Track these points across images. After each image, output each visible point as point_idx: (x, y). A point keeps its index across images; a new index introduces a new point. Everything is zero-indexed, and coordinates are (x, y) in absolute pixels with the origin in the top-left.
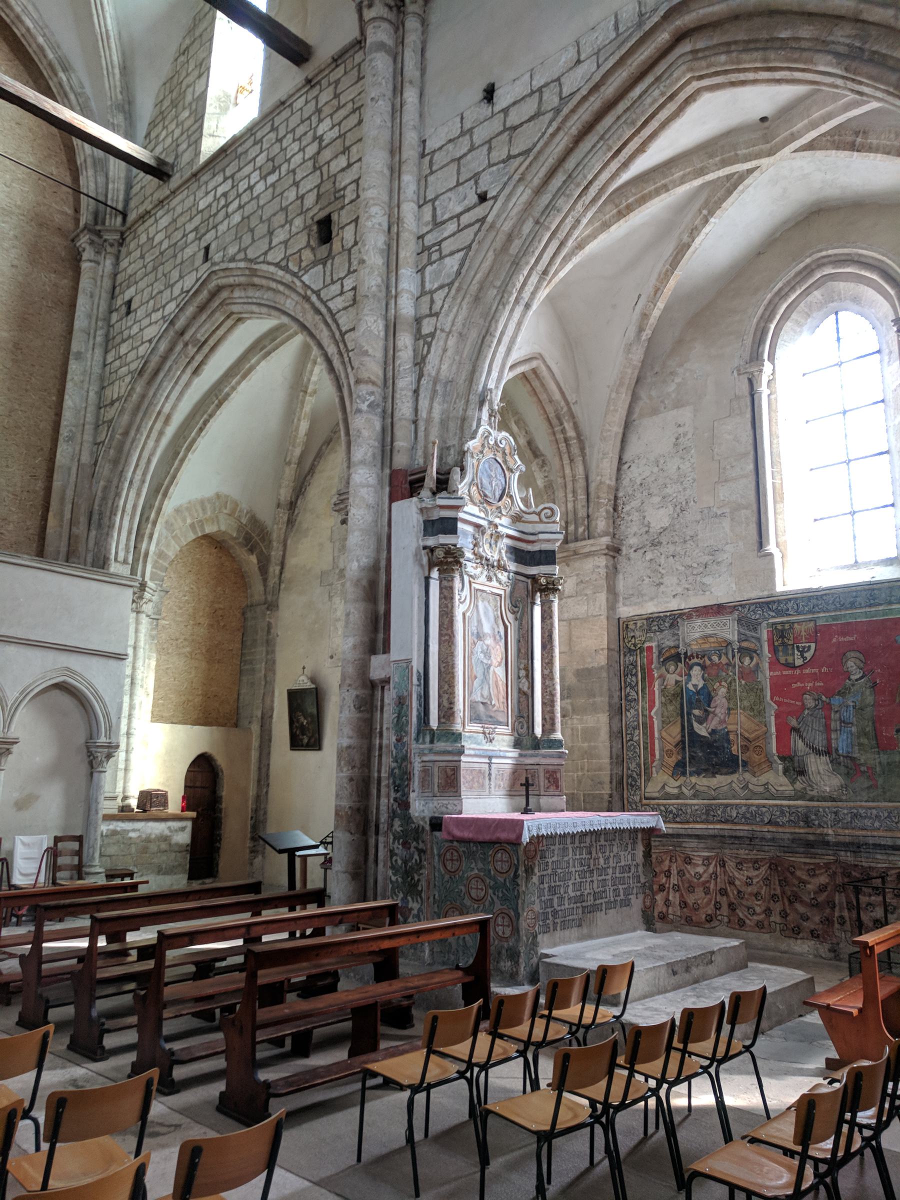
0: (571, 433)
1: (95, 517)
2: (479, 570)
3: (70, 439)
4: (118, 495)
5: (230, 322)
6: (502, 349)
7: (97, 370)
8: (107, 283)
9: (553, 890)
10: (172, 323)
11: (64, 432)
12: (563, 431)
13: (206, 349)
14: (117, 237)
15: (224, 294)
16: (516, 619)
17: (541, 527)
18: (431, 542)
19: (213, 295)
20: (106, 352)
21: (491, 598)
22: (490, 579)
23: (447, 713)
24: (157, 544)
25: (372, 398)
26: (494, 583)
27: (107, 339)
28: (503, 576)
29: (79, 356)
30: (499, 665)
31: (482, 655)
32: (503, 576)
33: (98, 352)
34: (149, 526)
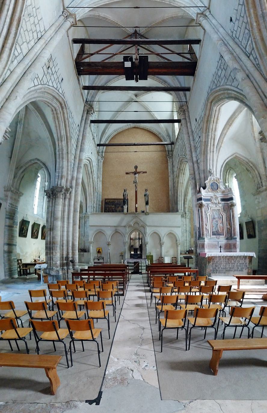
0: (251, 165)
1: (176, 203)
2: (213, 205)
3: (171, 190)
4: (178, 198)
5: (185, 165)
6: (211, 161)
7: (172, 178)
8: (171, 163)
9: (216, 266)
10: (178, 167)
11: (170, 189)
12: (250, 165)
13: (183, 170)
14: (171, 155)
15: (182, 161)
16: (225, 213)
17: (229, 193)
18: (198, 203)
19: (181, 162)
20: (173, 174)
21: (217, 211)
22: (216, 206)
23: (203, 234)
24: (188, 205)
25: (192, 177)
26: (218, 207)
27: (173, 172)
28: (221, 205)
29: (170, 176)
30: (221, 223)
31: (215, 222)
32: (221, 205)
33: (172, 175)
34: (186, 202)
